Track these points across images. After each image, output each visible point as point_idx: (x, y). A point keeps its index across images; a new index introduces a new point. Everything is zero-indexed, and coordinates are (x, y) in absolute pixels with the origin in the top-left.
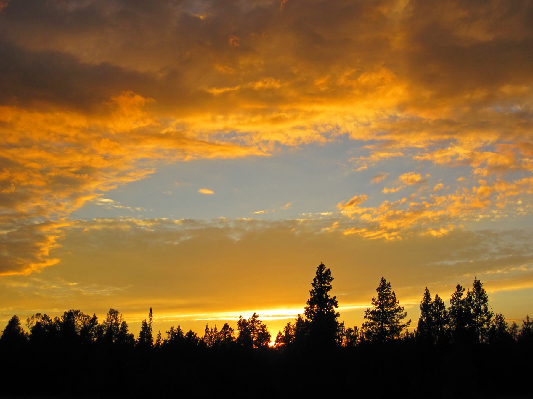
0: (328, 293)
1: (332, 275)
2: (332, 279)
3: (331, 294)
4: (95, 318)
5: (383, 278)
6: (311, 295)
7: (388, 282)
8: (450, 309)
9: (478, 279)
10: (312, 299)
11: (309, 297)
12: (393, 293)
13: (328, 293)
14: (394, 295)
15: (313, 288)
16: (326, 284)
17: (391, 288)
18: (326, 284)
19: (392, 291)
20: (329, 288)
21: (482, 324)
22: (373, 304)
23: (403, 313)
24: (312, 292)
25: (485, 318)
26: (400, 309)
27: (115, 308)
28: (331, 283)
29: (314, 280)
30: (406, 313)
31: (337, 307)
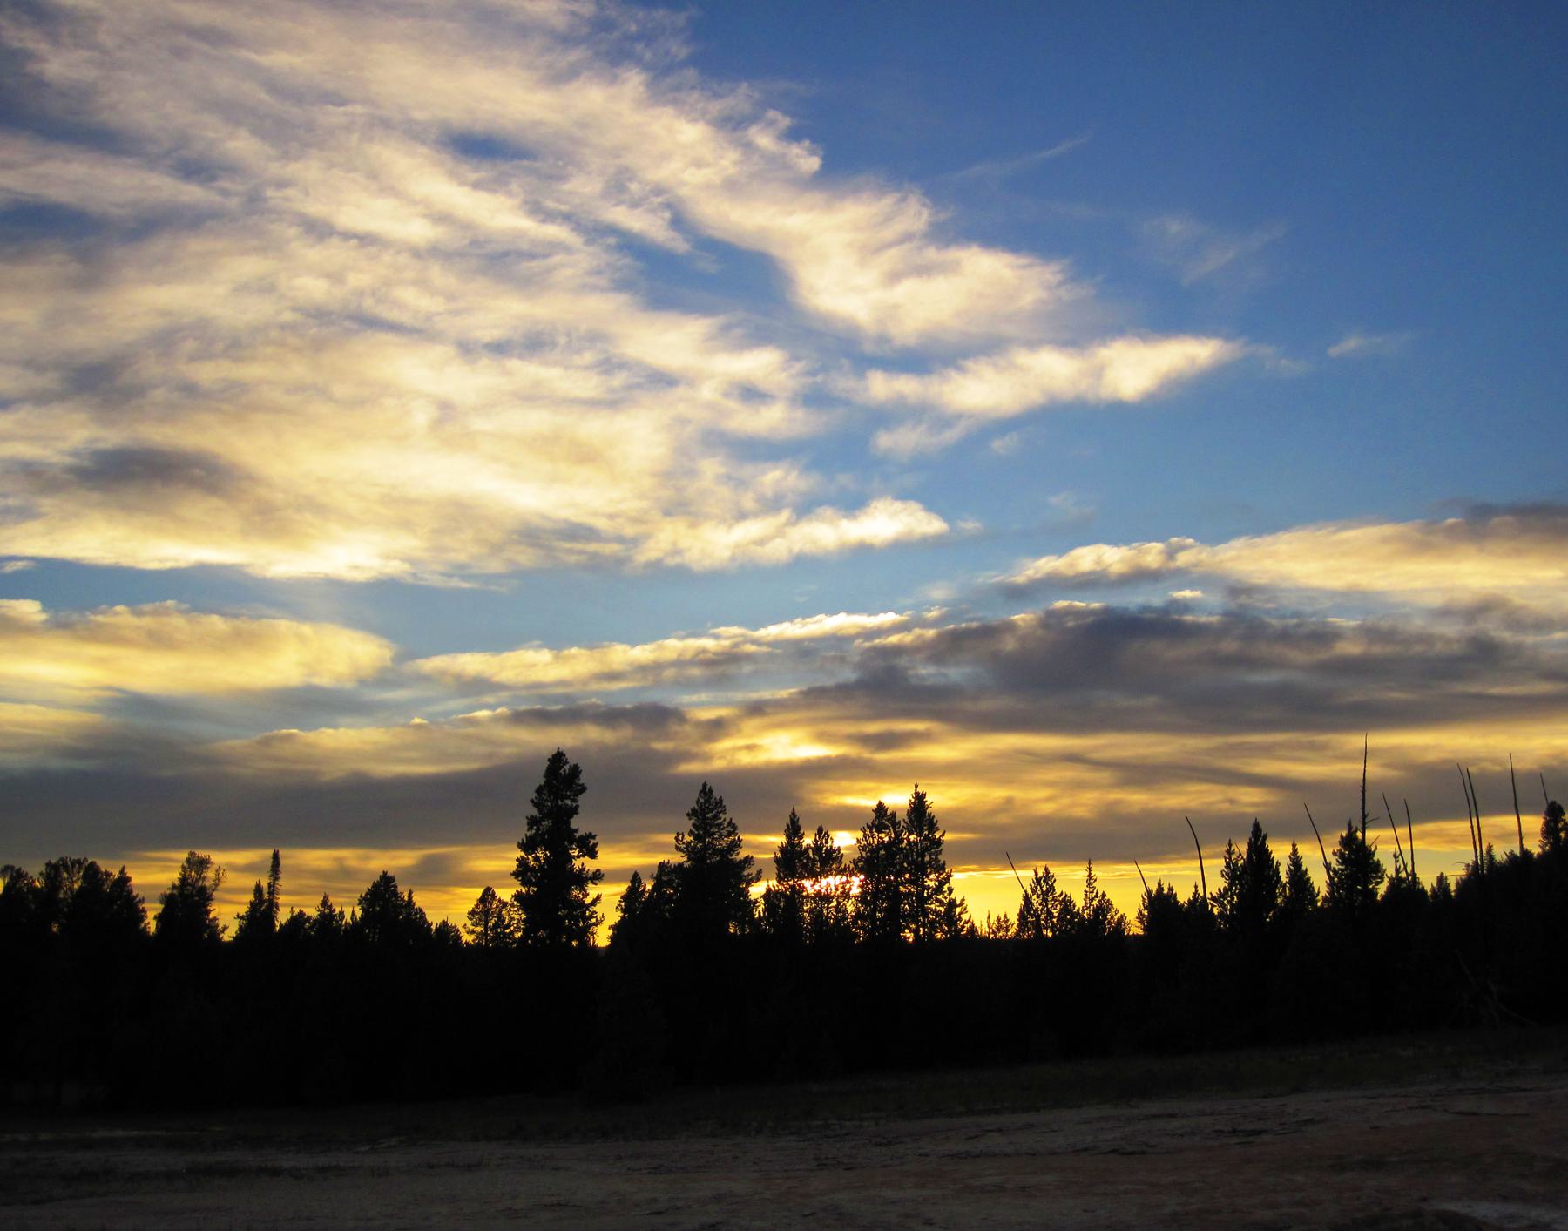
0: (575, 823)
1: (583, 779)
2: (584, 789)
3: (580, 824)
4: (124, 880)
5: (705, 785)
6: (530, 829)
7: (716, 795)
8: (855, 862)
9: (920, 790)
10: (530, 839)
11: (523, 832)
12: (730, 823)
13: (575, 823)
14: (735, 827)
15: (535, 812)
16: (568, 802)
17: (724, 812)
18: (568, 802)
19: (725, 817)
20: (575, 811)
21: (922, 901)
22: (678, 848)
23: (750, 871)
24: (532, 822)
25: (932, 884)
26: (748, 860)
27: (202, 853)
28: (582, 799)
29: (539, 791)
30: (760, 872)
31: (593, 854)
